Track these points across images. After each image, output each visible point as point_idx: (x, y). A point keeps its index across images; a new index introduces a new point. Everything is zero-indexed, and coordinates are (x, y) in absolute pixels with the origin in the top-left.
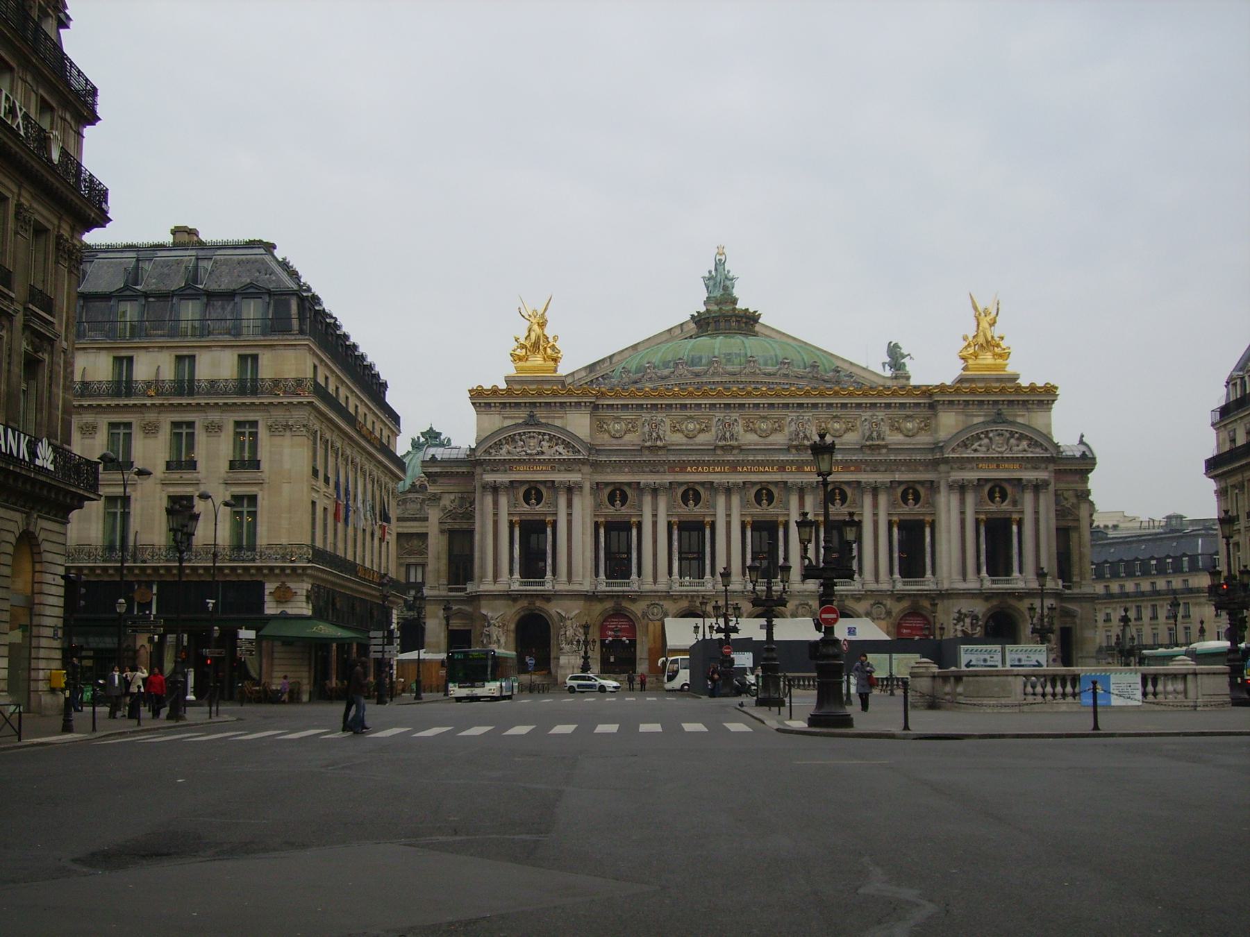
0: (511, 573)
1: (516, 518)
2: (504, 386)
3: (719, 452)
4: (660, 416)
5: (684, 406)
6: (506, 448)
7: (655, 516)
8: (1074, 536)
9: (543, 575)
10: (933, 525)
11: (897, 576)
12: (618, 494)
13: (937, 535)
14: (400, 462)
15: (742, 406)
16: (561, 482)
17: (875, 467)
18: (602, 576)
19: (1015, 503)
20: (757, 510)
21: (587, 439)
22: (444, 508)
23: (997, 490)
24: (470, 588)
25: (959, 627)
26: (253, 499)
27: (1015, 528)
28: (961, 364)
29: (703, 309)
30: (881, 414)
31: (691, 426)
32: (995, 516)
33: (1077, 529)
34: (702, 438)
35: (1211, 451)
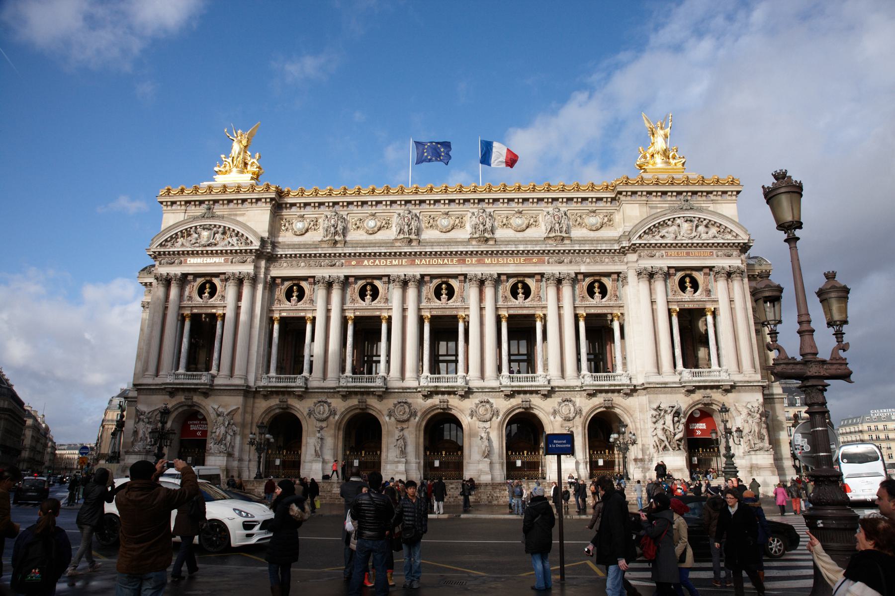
1: (187, 312)
3: (398, 244)
5: (364, 203)
6: (180, 240)
7: (328, 311)
11: (584, 370)
12: (296, 289)
16: (234, 274)
17: (558, 255)
19: (708, 292)
20: (437, 303)
21: (266, 235)
23: (688, 280)
25: (660, 425)
27: (710, 318)
30: (564, 208)
31: (372, 223)
32: (686, 306)
34: (381, 236)
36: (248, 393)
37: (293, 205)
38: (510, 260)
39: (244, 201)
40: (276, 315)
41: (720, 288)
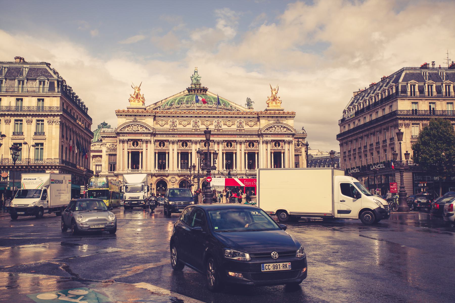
0: (128, 168)
2: (127, 110)
4: (175, 119)
5: (182, 117)
6: (127, 129)
8: (300, 157)
9: (138, 168)
10: (258, 153)
11: (247, 169)
12: (162, 143)
13: (260, 157)
14: (92, 134)
15: (200, 117)
17: (240, 135)
18: (157, 169)
19: (282, 147)
21: (152, 127)
22: (107, 147)
23: (277, 143)
24: (115, 172)
26: (42, 144)
28: (267, 105)
29: (190, 87)
30: (242, 120)
33: (301, 155)
34: (188, 127)
35: (338, 132)
36: (152, 175)
37: (160, 116)
38: (226, 136)
39: (145, 116)
40: (157, 151)
41: (286, 146)
